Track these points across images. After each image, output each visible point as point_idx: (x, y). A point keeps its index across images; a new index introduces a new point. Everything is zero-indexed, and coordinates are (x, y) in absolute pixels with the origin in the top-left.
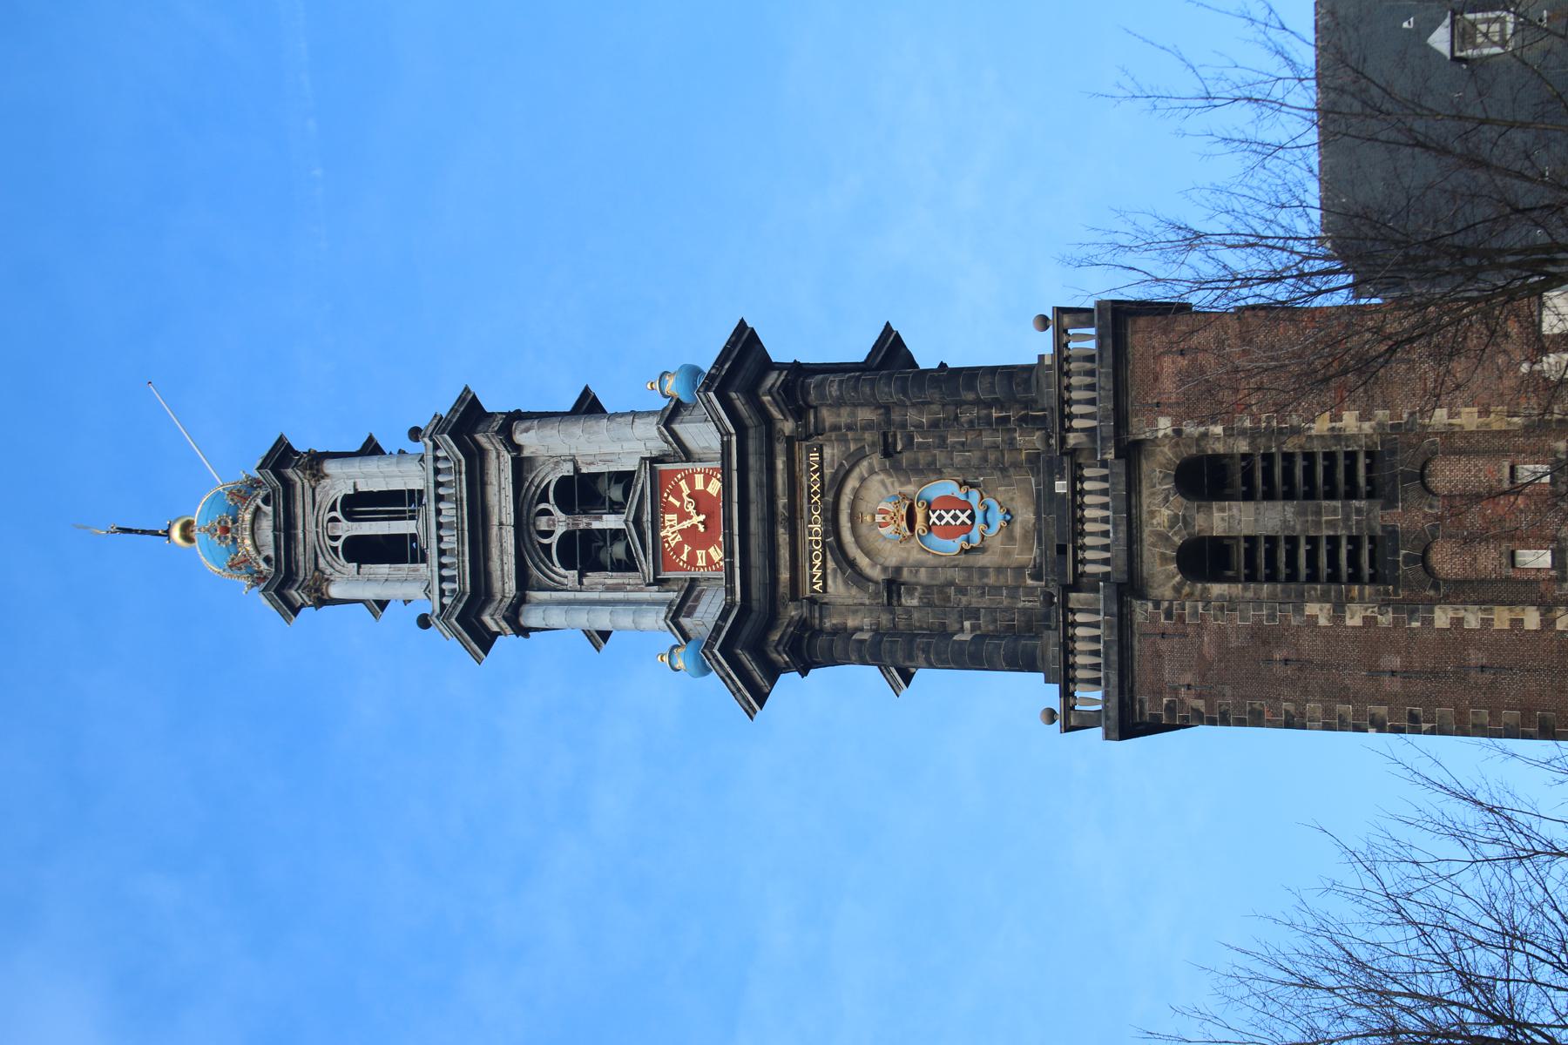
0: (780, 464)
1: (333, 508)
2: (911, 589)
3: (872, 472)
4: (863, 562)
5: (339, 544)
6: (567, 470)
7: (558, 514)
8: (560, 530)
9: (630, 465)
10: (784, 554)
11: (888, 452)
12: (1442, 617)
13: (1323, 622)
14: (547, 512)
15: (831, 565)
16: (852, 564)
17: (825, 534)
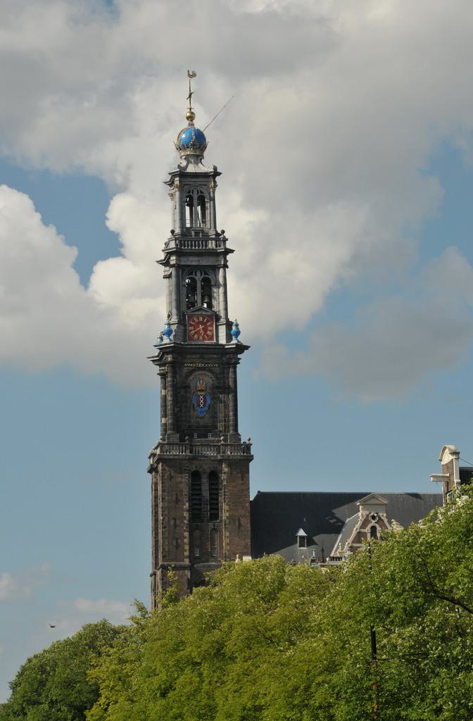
0: (215, 356)
1: (201, 192)
2: (186, 392)
3: (213, 381)
4: (191, 378)
5: (191, 194)
6: (213, 283)
7: (201, 278)
8: (197, 278)
9: (215, 309)
10: (194, 356)
11: (218, 388)
12: (186, 534)
13: (185, 507)
14: (201, 275)
15: (191, 368)
16: (191, 375)
17: (198, 368)
